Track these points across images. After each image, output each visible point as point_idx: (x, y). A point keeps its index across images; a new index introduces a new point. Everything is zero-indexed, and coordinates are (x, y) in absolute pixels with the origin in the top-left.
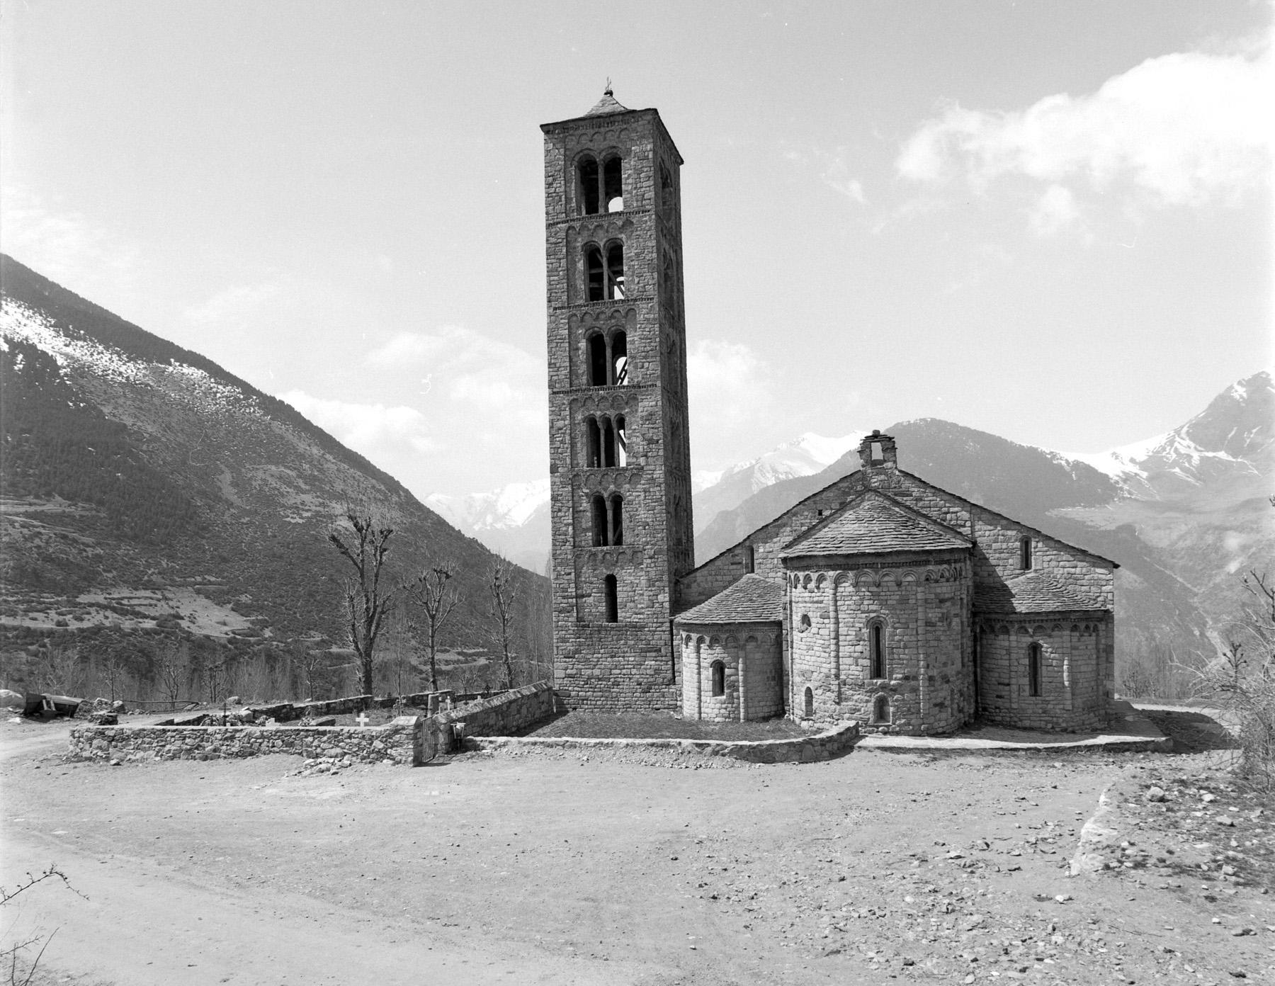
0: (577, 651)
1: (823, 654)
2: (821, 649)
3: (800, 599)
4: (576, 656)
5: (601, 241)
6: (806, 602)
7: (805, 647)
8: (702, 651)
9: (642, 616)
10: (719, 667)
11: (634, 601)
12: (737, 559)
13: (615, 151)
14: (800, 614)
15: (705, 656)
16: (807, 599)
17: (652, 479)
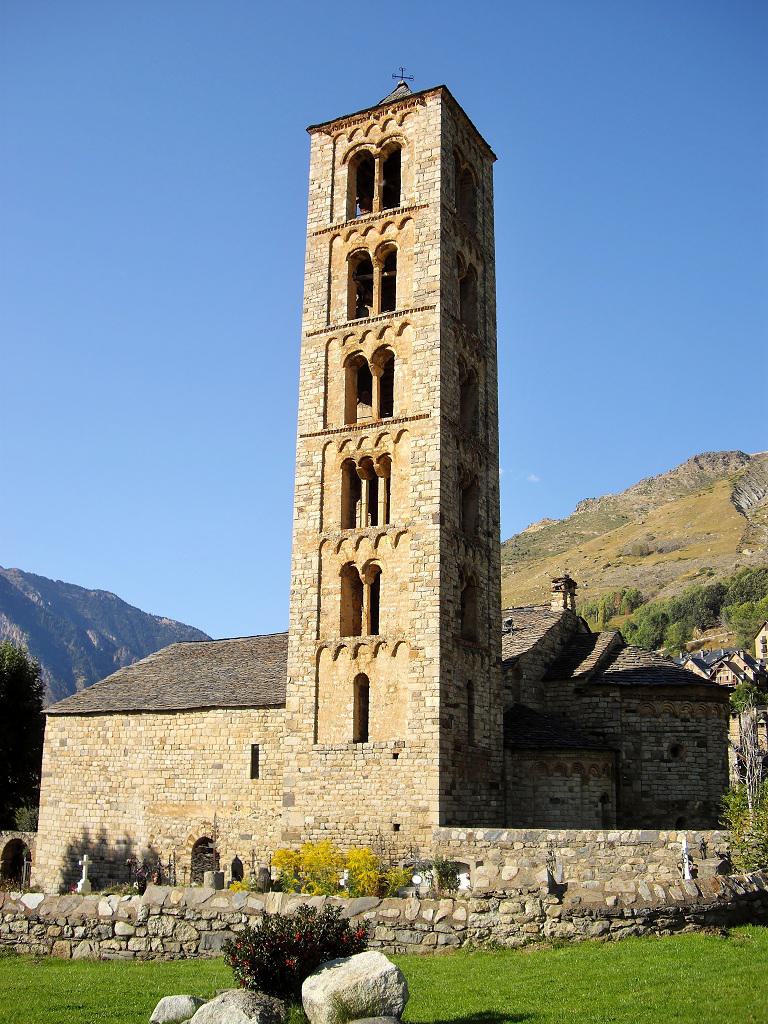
0: (453, 786)
1: (700, 782)
2: (698, 777)
3: (668, 729)
4: (454, 792)
5: (469, 258)
6: (677, 732)
7: (677, 777)
8: (591, 783)
9: (487, 741)
10: (604, 799)
11: (483, 720)
12: (509, 683)
13: (472, 171)
14: (666, 745)
15: (595, 789)
16: (682, 729)
17: (495, 569)
